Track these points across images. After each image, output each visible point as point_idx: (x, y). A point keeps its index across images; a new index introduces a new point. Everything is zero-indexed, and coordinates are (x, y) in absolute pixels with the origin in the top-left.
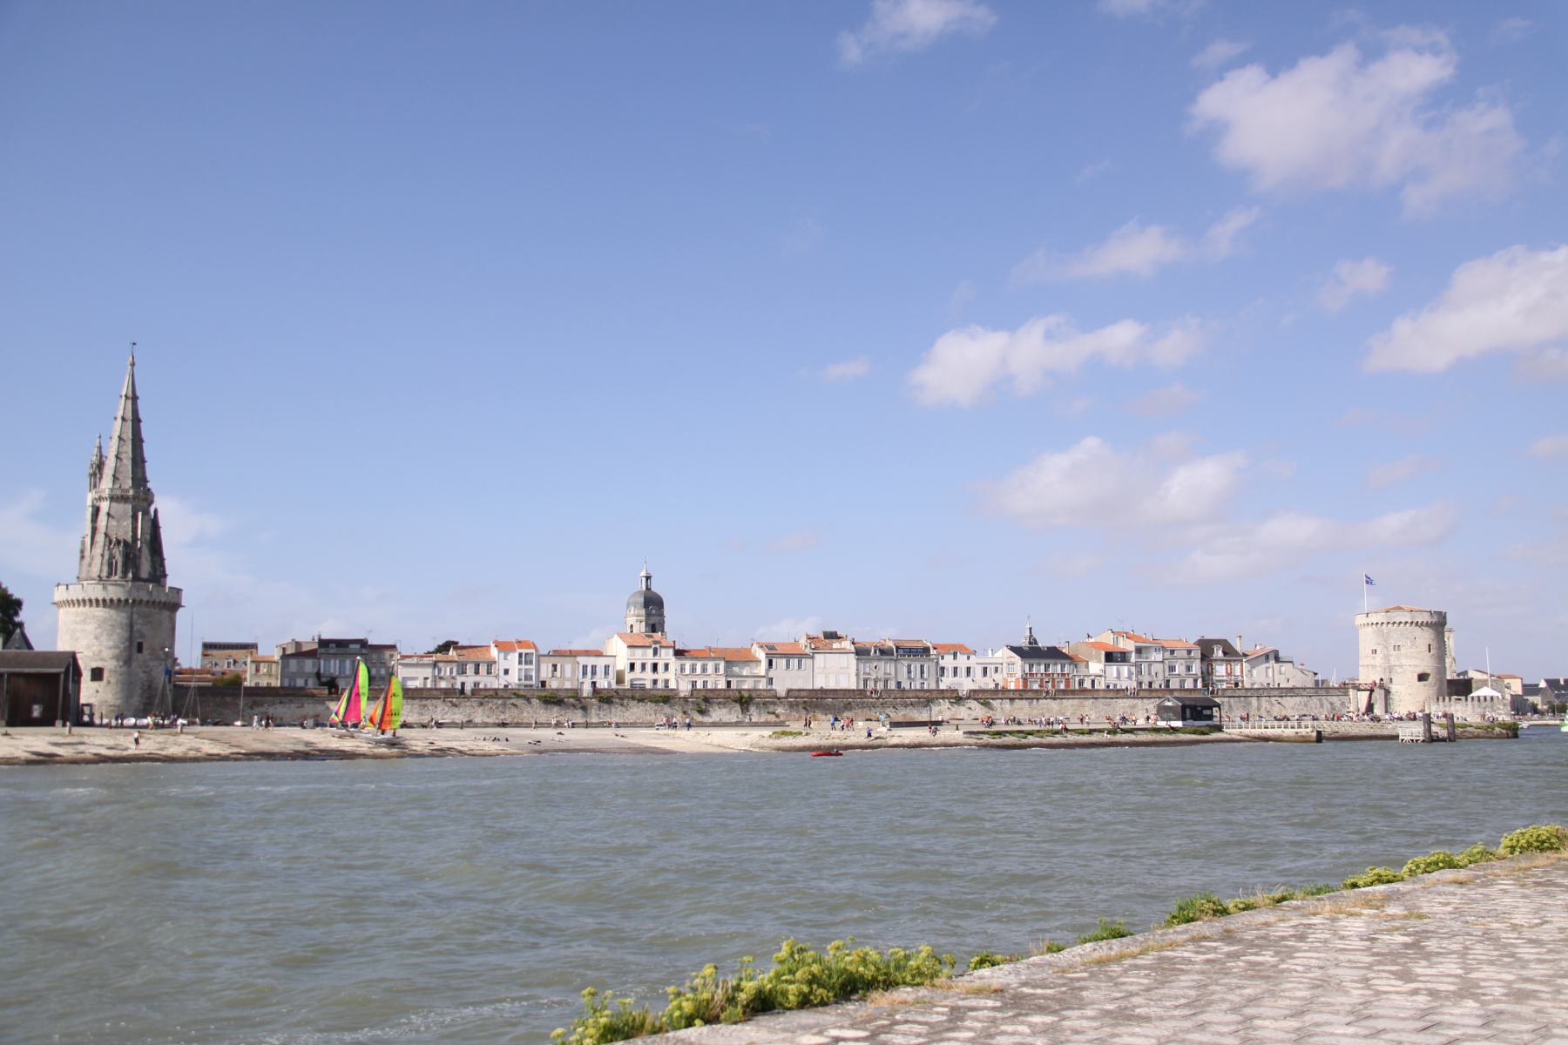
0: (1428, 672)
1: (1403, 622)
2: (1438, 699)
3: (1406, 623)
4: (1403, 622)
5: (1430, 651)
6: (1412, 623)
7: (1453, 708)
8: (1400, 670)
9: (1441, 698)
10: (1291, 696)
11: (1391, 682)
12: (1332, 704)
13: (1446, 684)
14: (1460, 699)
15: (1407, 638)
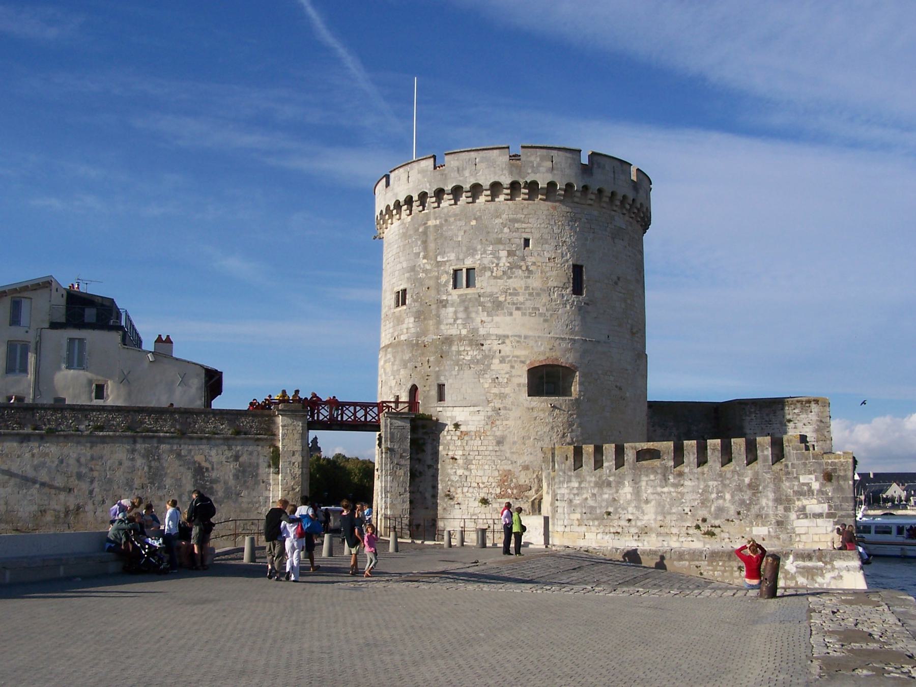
0: (566, 359)
1: (486, 183)
2: (578, 453)
3: (496, 188)
4: (486, 184)
5: (577, 290)
6: (514, 186)
7: (627, 490)
8: (471, 354)
9: (609, 449)
10: (25, 439)
11: (441, 398)
12: (199, 471)
13: (645, 408)
14: (654, 454)
15: (499, 242)
